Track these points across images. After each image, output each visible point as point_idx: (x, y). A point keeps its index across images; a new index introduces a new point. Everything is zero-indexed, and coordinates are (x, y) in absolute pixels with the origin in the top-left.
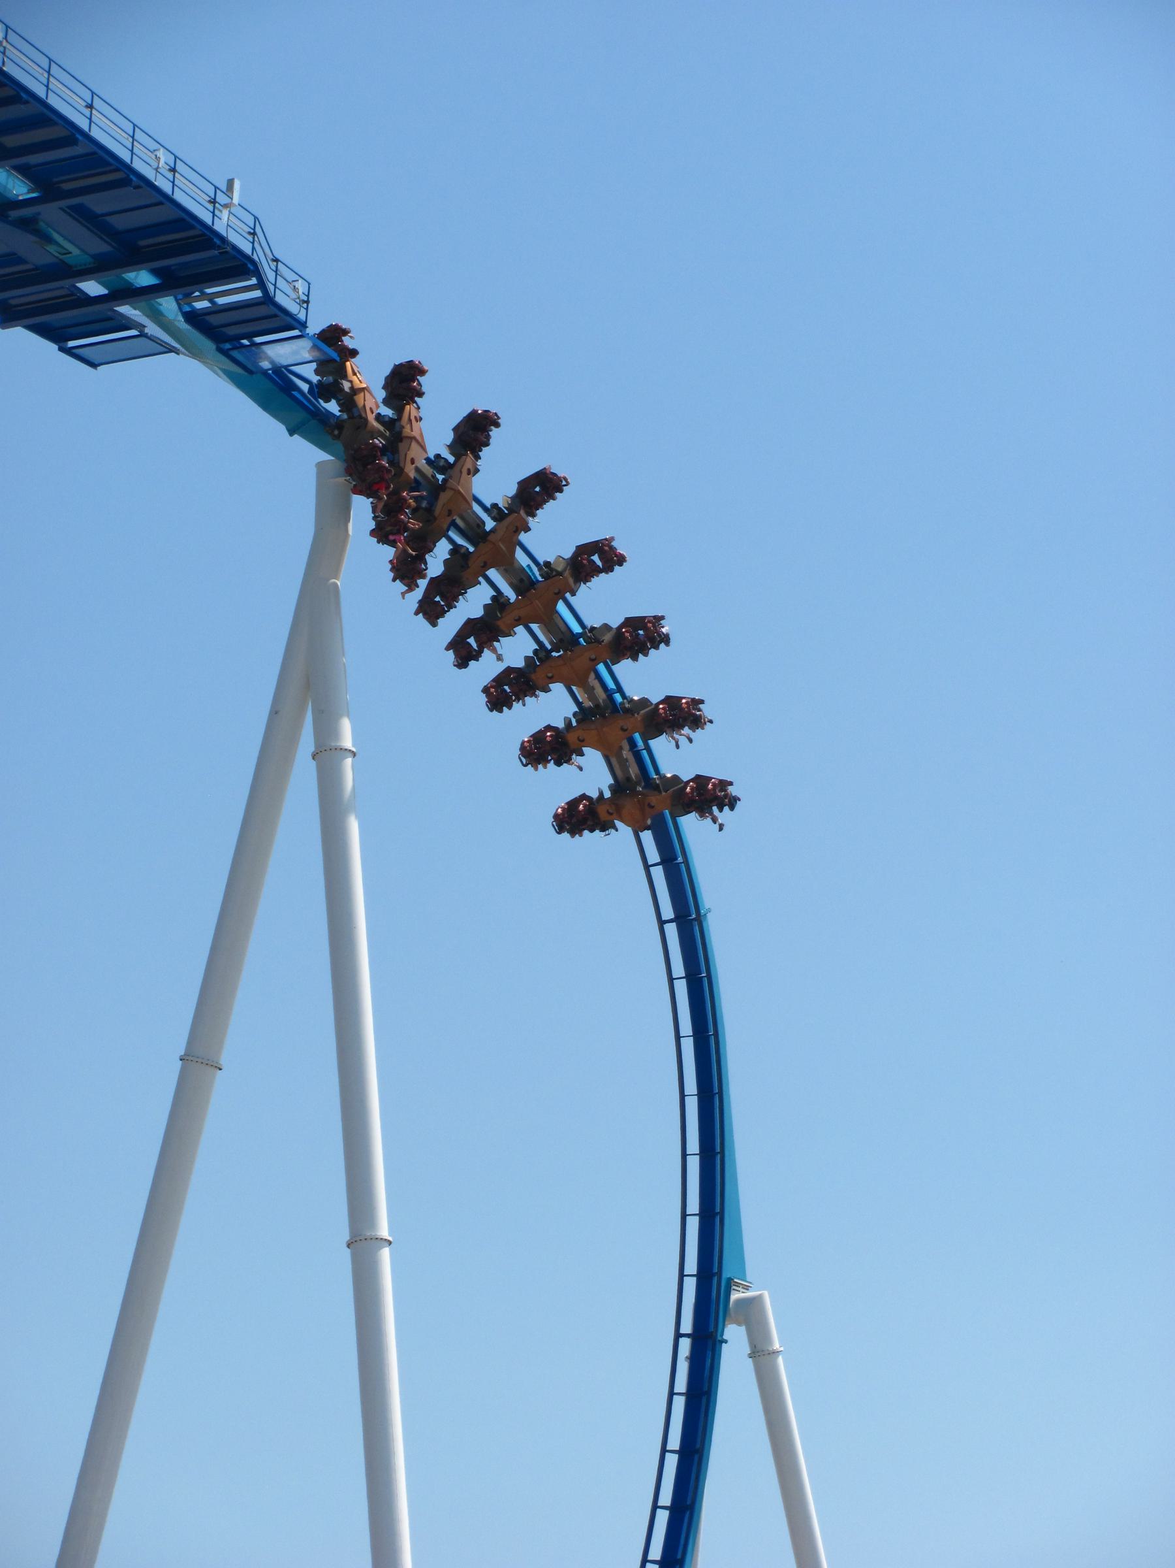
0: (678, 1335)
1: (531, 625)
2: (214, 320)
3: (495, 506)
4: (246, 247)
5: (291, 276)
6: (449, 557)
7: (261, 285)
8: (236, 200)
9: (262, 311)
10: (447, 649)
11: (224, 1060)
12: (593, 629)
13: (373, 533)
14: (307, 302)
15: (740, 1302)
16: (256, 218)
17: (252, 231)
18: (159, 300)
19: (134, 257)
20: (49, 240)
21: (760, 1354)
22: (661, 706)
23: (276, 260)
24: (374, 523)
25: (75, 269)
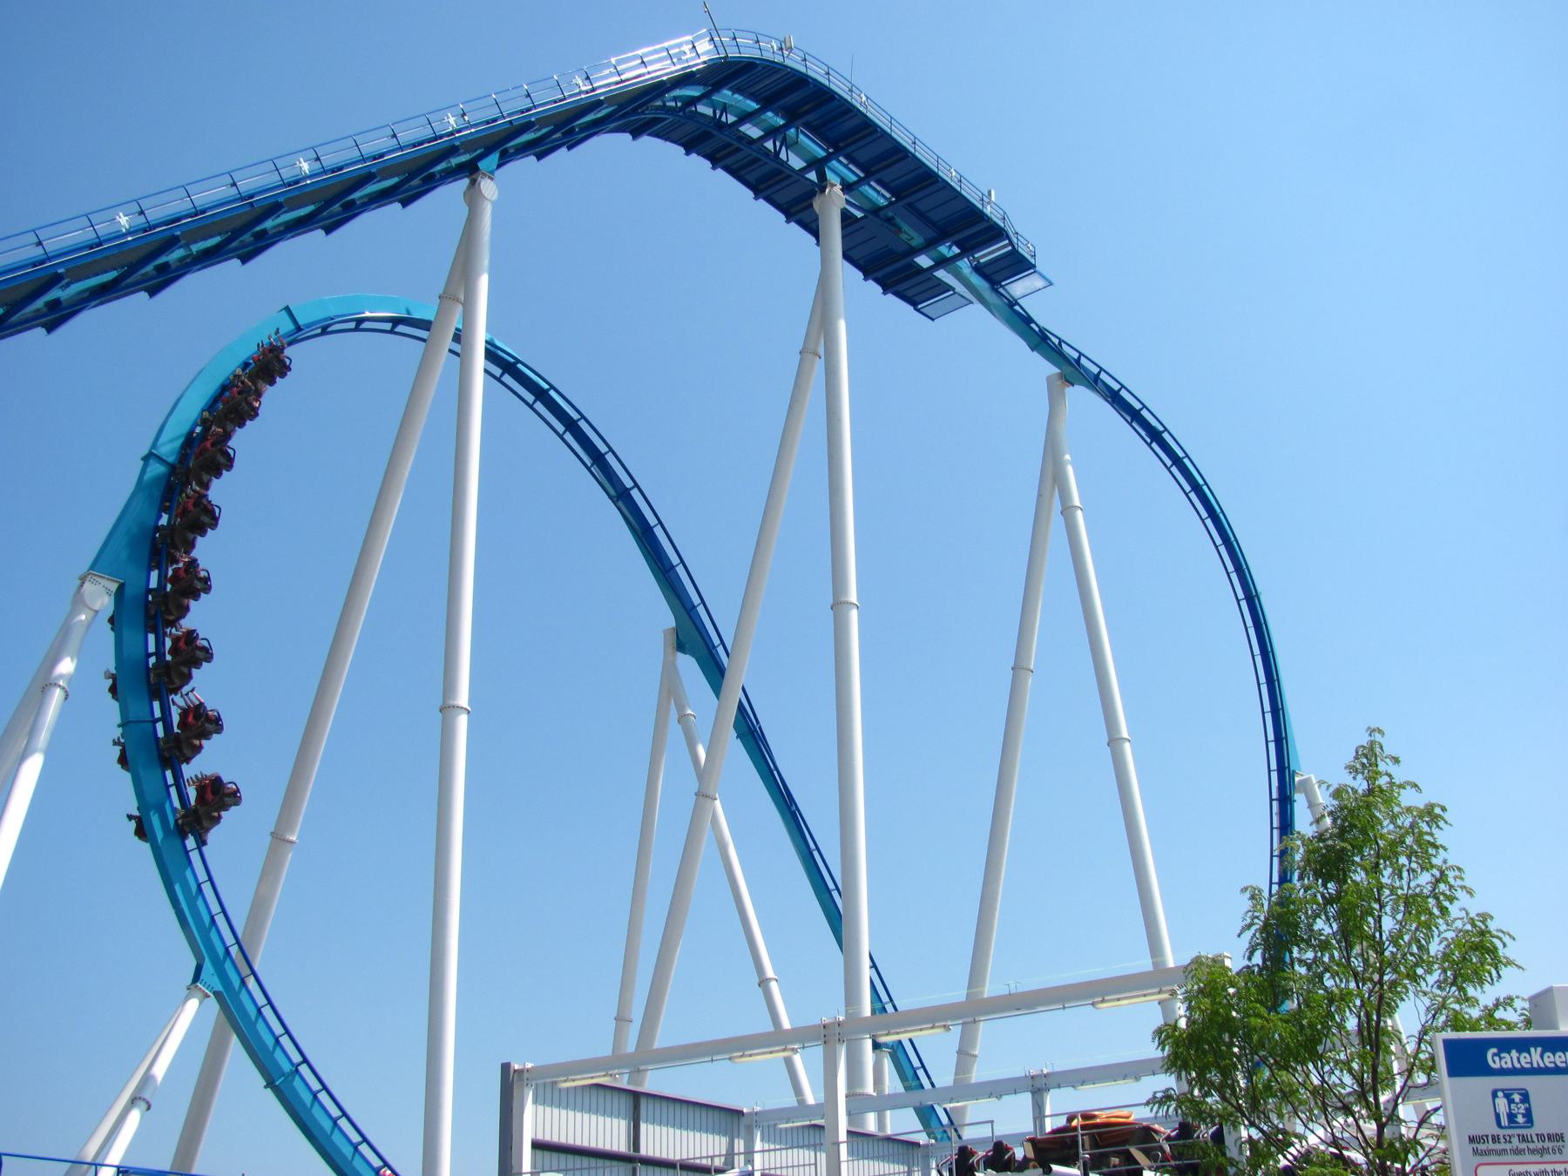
0: (1271, 800)
4: (1002, 225)
5: (1025, 242)
7: (1011, 243)
8: (993, 199)
15: (1300, 782)
18: (958, 263)
20: (899, 229)
23: (1017, 233)
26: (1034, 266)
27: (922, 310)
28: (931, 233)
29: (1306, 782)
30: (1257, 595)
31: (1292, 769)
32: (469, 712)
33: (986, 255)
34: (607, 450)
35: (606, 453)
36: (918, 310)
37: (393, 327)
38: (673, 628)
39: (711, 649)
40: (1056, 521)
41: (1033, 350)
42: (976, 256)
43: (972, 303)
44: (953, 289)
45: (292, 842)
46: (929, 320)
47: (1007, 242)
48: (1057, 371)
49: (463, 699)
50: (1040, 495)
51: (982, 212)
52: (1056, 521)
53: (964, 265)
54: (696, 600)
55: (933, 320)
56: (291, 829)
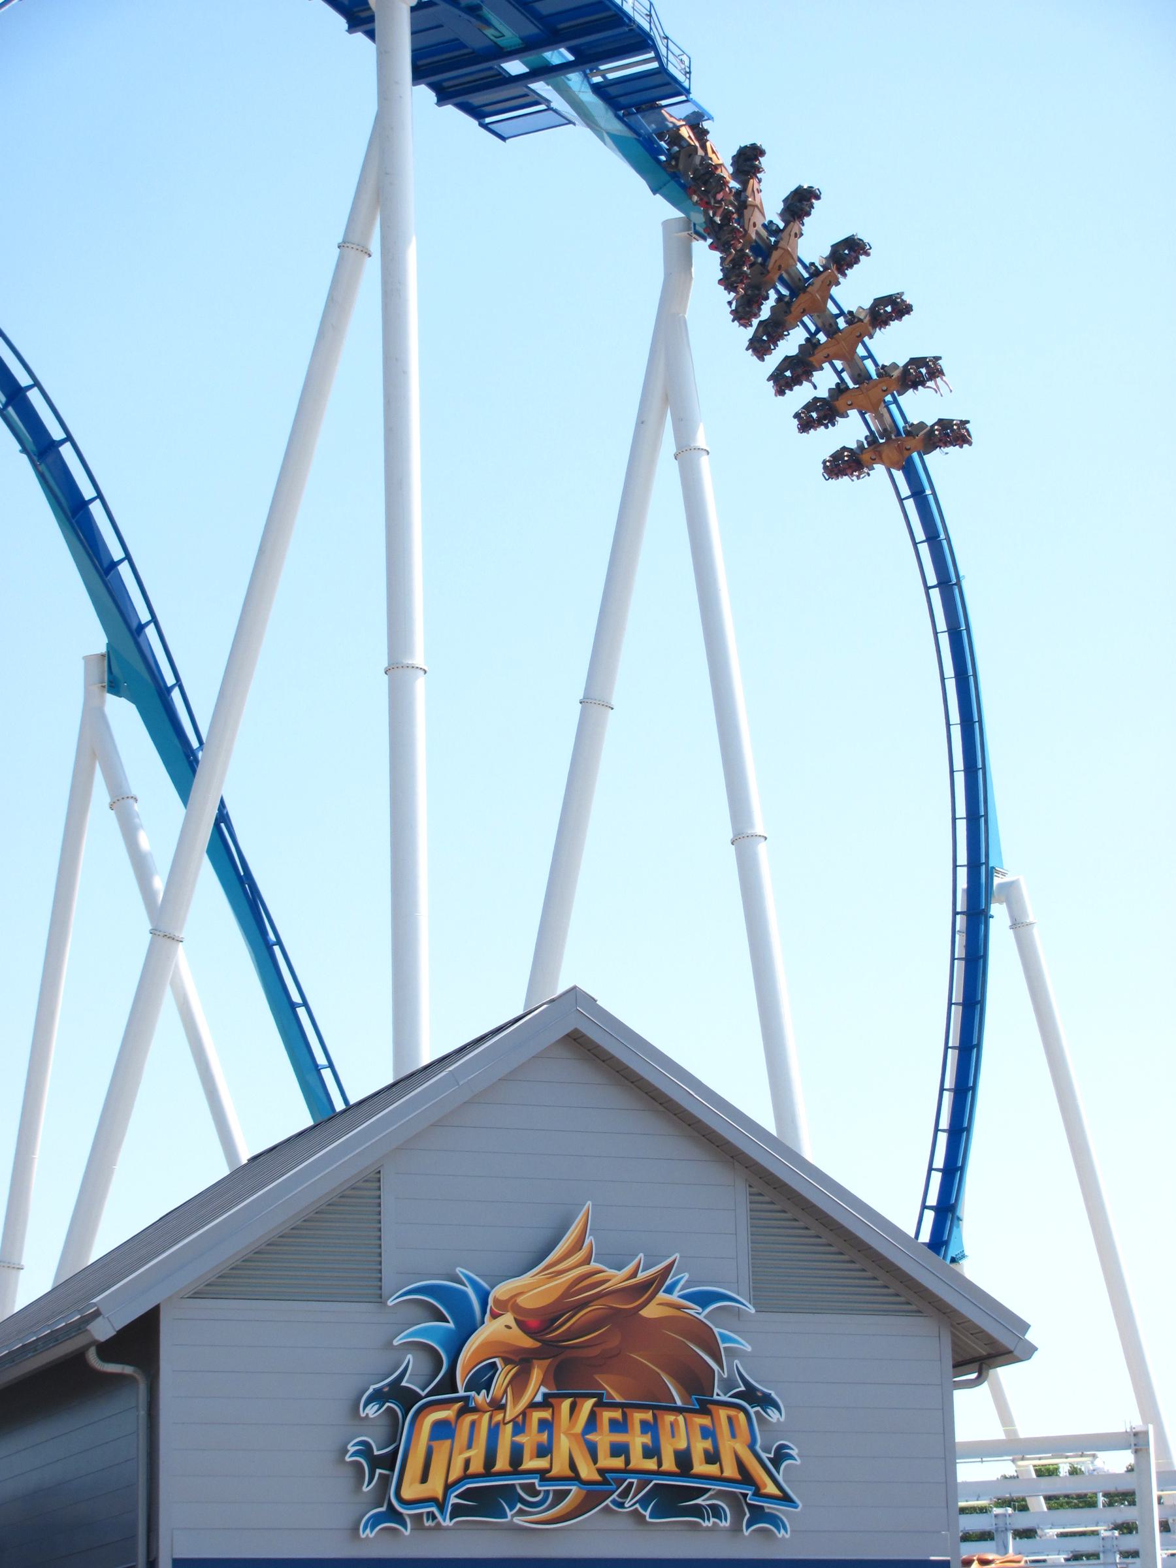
0: (955, 913)
1: (834, 361)
2: (612, 91)
3: (812, 264)
4: (646, 26)
5: (678, 52)
6: (775, 304)
7: (658, 57)
9: (657, 80)
10: (769, 380)
11: (614, 703)
12: (884, 367)
13: (720, 282)
14: (690, 73)
15: (1001, 885)
16: (651, 4)
17: (648, 13)
19: (553, 39)
20: (488, 24)
21: (1018, 925)
22: (936, 427)
23: (667, 38)
24: (722, 274)
25: (506, 50)
26: (688, 91)
28: (531, 29)
29: (1011, 887)
30: (958, 583)
31: (991, 865)
33: (617, 70)
34: (30, 382)
35: (29, 388)
38: (103, 655)
39: (164, 693)
40: (666, 471)
41: (655, 192)
42: (602, 67)
43: (570, 122)
44: (547, 102)
46: (500, 141)
47: (652, 55)
48: (680, 215)
50: (641, 422)
51: (620, 9)
52: (666, 471)
53: (575, 79)
55: (503, 139)
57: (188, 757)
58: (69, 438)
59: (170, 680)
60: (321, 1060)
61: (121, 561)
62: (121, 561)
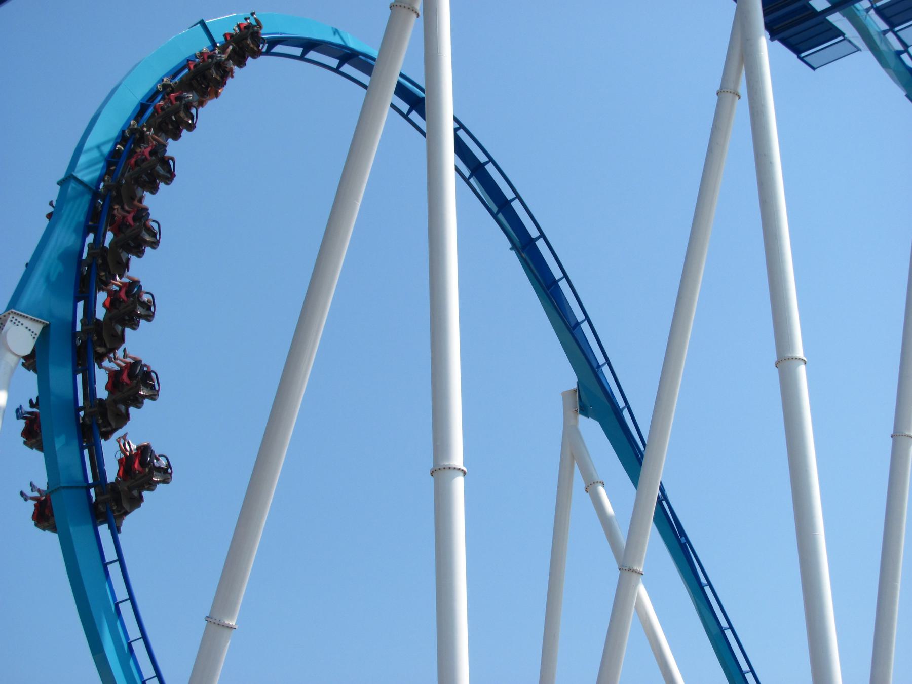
27: (805, 59)
32: (465, 473)
36: (802, 59)
37: (304, 53)
38: (575, 391)
39: (617, 412)
45: (231, 628)
49: (458, 460)
54: (601, 360)
55: (814, 69)
56: (230, 613)
57: (637, 455)
58: (542, 235)
59: (621, 404)
60: (745, 667)
61: (583, 321)
62: (583, 321)
